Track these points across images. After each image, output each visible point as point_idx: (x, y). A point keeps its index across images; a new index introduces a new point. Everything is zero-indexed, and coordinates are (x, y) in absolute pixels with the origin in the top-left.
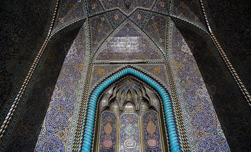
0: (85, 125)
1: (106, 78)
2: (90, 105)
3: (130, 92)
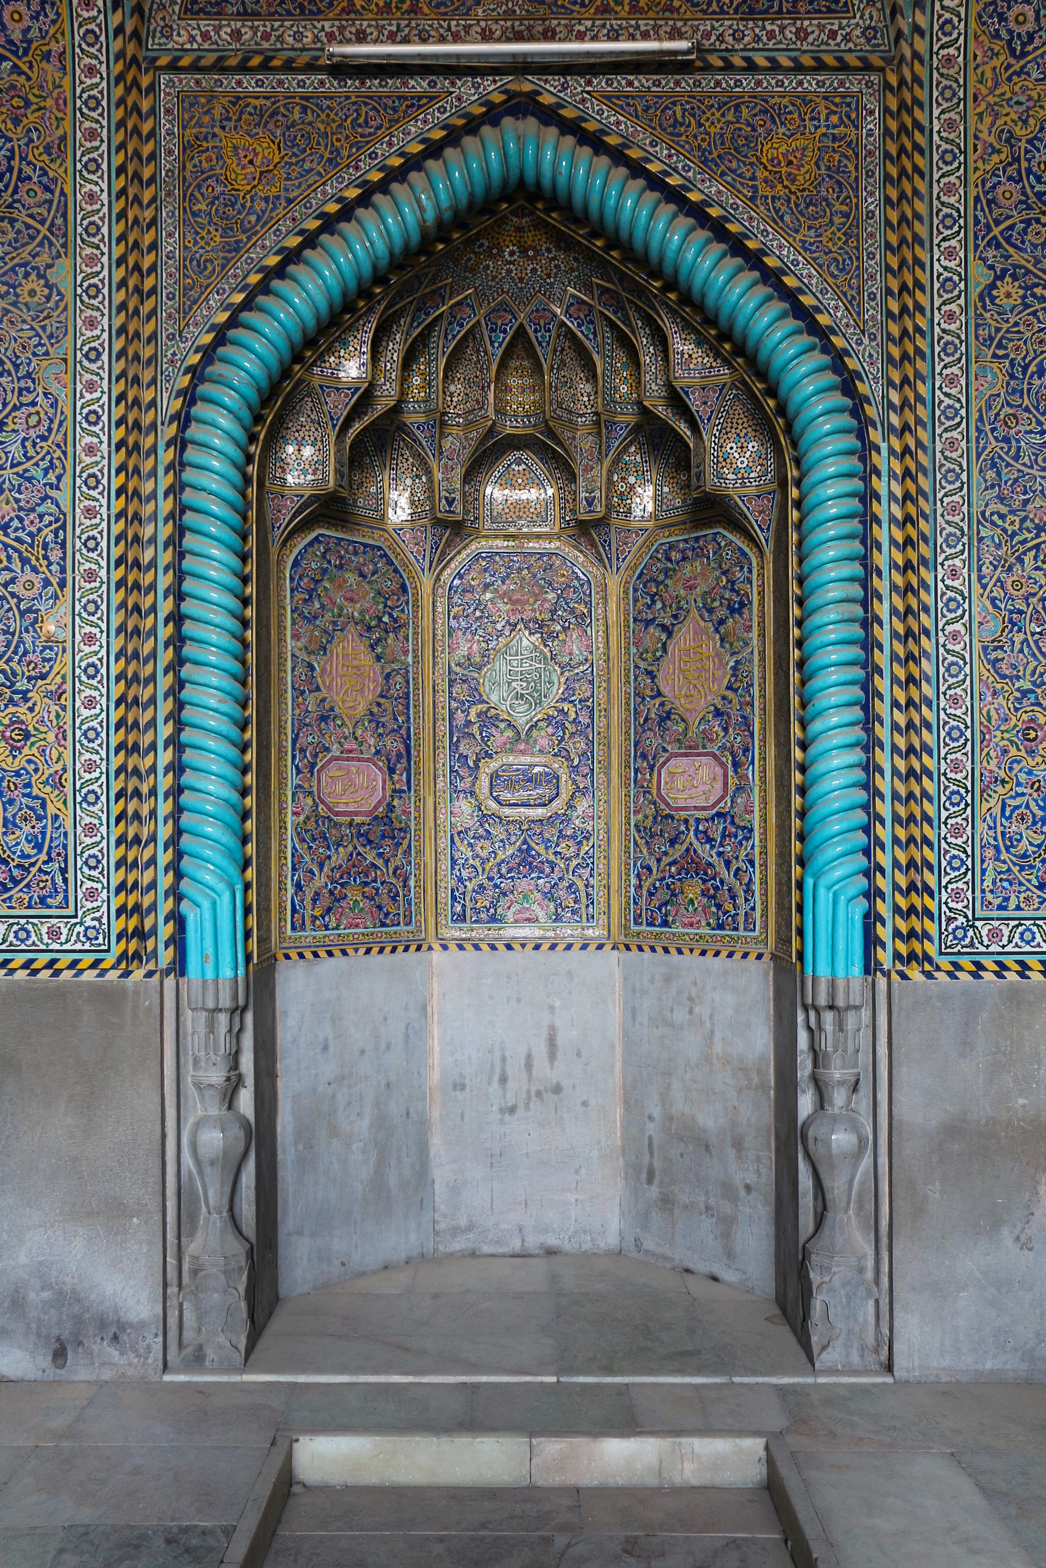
0: (178, 662)
2: (189, 518)
3: (532, 355)
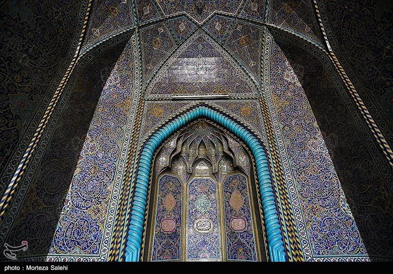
1: (167, 123)
2: (140, 164)
3: (204, 145)
